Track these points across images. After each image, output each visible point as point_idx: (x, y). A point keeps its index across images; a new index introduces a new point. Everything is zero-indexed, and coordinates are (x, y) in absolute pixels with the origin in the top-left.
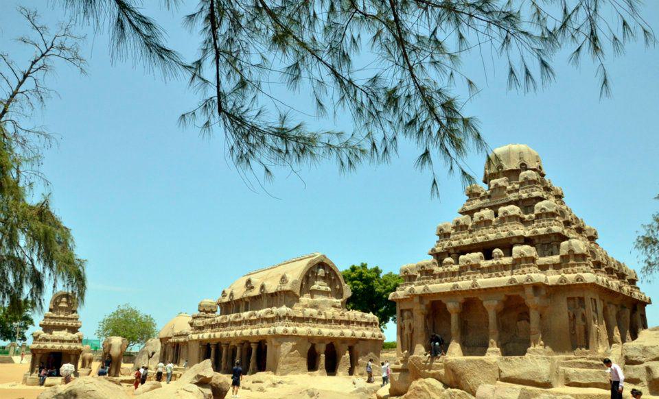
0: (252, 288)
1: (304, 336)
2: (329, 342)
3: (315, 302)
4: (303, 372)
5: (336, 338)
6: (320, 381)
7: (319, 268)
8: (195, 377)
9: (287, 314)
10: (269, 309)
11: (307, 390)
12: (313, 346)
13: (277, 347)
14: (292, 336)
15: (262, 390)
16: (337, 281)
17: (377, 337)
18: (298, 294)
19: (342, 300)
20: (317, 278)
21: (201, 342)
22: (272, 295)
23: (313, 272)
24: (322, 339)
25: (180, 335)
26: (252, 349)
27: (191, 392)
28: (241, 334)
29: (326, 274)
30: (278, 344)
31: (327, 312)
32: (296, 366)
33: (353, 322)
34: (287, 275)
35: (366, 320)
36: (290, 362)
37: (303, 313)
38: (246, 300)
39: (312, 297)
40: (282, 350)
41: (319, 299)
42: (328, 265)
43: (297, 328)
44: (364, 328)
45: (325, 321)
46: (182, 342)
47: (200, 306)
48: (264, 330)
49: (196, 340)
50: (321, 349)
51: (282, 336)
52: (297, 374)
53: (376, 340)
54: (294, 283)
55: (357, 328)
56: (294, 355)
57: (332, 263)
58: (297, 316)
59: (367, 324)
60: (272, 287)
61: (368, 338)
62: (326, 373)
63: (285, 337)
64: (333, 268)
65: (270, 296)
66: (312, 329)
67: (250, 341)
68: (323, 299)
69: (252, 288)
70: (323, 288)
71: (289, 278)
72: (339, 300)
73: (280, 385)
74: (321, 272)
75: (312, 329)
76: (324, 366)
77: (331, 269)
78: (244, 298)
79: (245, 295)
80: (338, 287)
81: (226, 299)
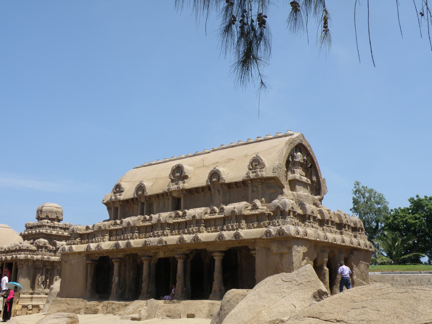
20: (295, 164)
21: (88, 254)
22: (230, 186)
30: (286, 250)
38: (175, 195)
39: (293, 189)
40: (295, 259)
45: (322, 222)
46: (22, 260)
47: (40, 211)
49: (80, 253)
53: (367, 251)
57: (309, 146)
64: (311, 152)
65: (226, 188)
67: (209, 249)
68: (305, 194)
69: (186, 177)
70: (304, 179)
74: (299, 157)
78: (171, 192)
79: (174, 187)
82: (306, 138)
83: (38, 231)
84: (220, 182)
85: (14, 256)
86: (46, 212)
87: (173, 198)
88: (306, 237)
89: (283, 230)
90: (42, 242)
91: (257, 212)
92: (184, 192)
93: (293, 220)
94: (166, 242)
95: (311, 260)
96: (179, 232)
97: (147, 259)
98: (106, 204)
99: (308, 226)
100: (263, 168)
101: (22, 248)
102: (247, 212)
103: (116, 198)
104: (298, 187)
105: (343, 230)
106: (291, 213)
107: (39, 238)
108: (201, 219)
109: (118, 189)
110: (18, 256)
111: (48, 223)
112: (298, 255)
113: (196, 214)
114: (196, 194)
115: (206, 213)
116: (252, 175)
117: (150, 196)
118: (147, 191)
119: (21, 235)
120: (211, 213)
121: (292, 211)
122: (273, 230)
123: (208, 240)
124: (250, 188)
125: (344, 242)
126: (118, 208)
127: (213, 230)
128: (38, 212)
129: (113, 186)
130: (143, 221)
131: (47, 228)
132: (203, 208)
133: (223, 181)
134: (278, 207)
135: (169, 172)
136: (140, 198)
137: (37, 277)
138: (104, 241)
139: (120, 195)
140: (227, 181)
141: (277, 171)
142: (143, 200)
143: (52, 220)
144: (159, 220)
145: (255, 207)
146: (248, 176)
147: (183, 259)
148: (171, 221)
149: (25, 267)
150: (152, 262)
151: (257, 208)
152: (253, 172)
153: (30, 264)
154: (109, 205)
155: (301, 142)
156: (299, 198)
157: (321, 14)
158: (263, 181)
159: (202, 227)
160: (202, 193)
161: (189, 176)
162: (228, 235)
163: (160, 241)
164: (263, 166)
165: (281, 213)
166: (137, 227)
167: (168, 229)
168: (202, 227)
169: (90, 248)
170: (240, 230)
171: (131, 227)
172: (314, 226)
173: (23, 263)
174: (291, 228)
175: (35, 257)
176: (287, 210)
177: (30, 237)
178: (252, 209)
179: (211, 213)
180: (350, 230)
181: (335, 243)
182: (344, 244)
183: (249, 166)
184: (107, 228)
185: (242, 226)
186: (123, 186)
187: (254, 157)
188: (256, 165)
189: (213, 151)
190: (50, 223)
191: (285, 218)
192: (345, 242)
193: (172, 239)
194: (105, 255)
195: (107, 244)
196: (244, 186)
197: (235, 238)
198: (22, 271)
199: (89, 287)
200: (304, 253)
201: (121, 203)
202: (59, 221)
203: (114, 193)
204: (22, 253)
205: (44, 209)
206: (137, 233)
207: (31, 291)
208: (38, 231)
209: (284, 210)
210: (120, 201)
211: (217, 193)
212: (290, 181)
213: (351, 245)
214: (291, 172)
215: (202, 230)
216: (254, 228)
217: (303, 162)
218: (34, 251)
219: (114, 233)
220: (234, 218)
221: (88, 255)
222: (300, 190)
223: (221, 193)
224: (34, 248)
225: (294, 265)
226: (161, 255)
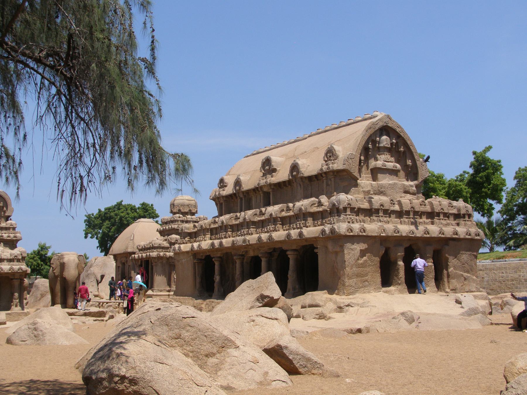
0: (274, 170)
1: (375, 237)
3: (382, 186)
4: (376, 290)
6: (397, 300)
7: (381, 135)
8: (258, 300)
9: (349, 204)
10: (313, 199)
11: (403, 314)
13: (336, 253)
14: (359, 236)
15: (322, 317)
16: (408, 155)
17: (473, 236)
18: (356, 174)
19: (416, 182)
20: (380, 150)
21: (194, 254)
22: (310, 178)
23: (374, 142)
25: (149, 248)
26: (289, 259)
27: (276, 319)
28: (270, 237)
29: (392, 144)
30: (338, 249)
31: (403, 201)
32: (367, 281)
33: (438, 214)
34: (336, 147)
35: (455, 211)
36: (358, 276)
37: (370, 202)
38: (265, 190)
39: (375, 179)
40: (347, 257)
41: (385, 180)
42: (394, 131)
43: (366, 225)
44: (454, 222)
45: (400, 214)
47: (173, 205)
48: (311, 231)
49: (187, 252)
51: (346, 236)
52: (369, 292)
53: (472, 240)
54: (350, 158)
55: (444, 222)
56: (363, 265)
57: (399, 127)
58: (362, 206)
59: (457, 216)
60: (310, 166)
62: (406, 290)
65: (307, 181)
66: (386, 226)
67: (285, 247)
68: (391, 182)
69: (274, 170)
70: (390, 165)
71: (339, 151)
72: (412, 183)
74: (385, 140)
75: (386, 226)
76: (403, 279)
77: (398, 136)
78: (261, 187)
79: (263, 182)
80: (409, 162)
81: (229, 190)
82: (393, 119)
83: (170, 226)
84: (299, 176)
85: (148, 254)
86: (178, 206)
87: (264, 193)
88: (364, 234)
89: (334, 228)
90: (174, 239)
91: (321, 209)
92: (272, 187)
93: (351, 216)
94: (249, 241)
95: (375, 256)
96: (262, 230)
97: (239, 257)
98: (213, 199)
99: (374, 221)
100: (336, 159)
101: (154, 245)
102: (315, 209)
103: (219, 194)
104: (380, 176)
105: (436, 220)
106: (348, 210)
107: (171, 234)
108: (277, 218)
109: (222, 184)
110: (151, 254)
111: (179, 217)
112: (353, 252)
113: (273, 212)
114: (285, 187)
115: (283, 210)
116: (325, 168)
117: (248, 190)
118: (243, 186)
119: (157, 231)
120: (287, 211)
121: (349, 207)
122: (327, 228)
123: (280, 240)
124: (325, 183)
125: (428, 234)
126: (226, 203)
127: (287, 228)
128: (171, 205)
129: (218, 181)
130: (235, 219)
131: (179, 223)
132: (280, 205)
133: (302, 175)
134: (334, 205)
135: (260, 165)
136: (238, 193)
137: (173, 274)
138: (205, 240)
139: (224, 190)
140: (306, 174)
141: (347, 163)
142: (241, 196)
143: (185, 214)
144: (245, 219)
145: (320, 204)
146: (321, 169)
147: (266, 257)
148: (257, 219)
149: (159, 264)
150: (245, 260)
151: (322, 205)
152: (327, 165)
153: (164, 262)
154: (217, 199)
155: (385, 124)
156: (379, 188)
157: (17, 185)
158: (335, 174)
159: (278, 225)
160: (289, 186)
161: (278, 169)
162: (294, 233)
163: (244, 241)
164: (336, 157)
165: (336, 211)
166: (230, 225)
167: (253, 228)
168: (278, 225)
169: (194, 248)
170: (304, 228)
171: (225, 226)
172: (382, 220)
173: (156, 261)
174: (342, 227)
175: (168, 254)
176: (341, 207)
177: (166, 233)
178: (318, 206)
179: (287, 211)
180: (452, 218)
181: (413, 235)
182: (428, 236)
183: (324, 157)
184: (208, 227)
185: (308, 225)
186: (226, 181)
187: (329, 148)
188: (330, 157)
189: (309, 136)
190: (183, 218)
191: (339, 216)
192: (430, 233)
193: (253, 238)
194: (208, 254)
195: (205, 243)
196: (318, 180)
197: (300, 237)
198: (158, 268)
199: (198, 285)
200: (361, 250)
201: (225, 199)
202: (193, 214)
203: (220, 188)
204: (155, 250)
205: (176, 202)
206: (230, 231)
207: (168, 289)
208: (170, 226)
209: (339, 207)
210: (223, 197)
211: (299, 187)
212: (371, 170)
213: (440, 235)
214: (375, 159)
215: (277, 229)
216: (319, 226)
217: (389, 146)
218: (167, 248)
219: (214, 231)
220: (302, 216)
221: (195, 254)
222: (385, 178)
223: (302, 186)
224: (166, 244)
225: (347, 263)
226: (251, 254)
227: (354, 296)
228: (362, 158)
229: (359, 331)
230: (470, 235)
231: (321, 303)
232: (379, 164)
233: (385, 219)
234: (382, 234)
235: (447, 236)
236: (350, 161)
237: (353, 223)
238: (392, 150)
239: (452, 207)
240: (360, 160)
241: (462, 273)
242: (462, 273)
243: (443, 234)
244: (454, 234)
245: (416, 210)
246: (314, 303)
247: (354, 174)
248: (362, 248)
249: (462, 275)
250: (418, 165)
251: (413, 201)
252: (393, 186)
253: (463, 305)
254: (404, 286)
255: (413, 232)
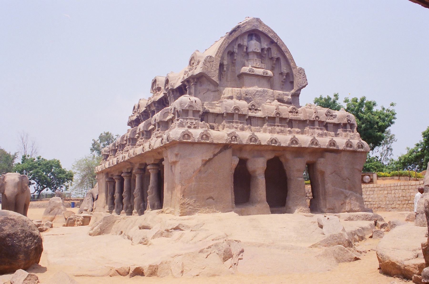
2: (270, 156)
5: (285, 149)
9: (190, 106)
12: (243, 162)
16: (282, 61)
18: (215, 78)
24: (258, 149)
29: (262, 50)
42: (266, 36)
44: (333, 133)
50: (258, 166)
53: (354, 152)
55: (320, 132)
61: (341, 148)
62: (269, 209)
63: (185, 144)
66: (239, 133)
68: (260, 89)
69: (159, 89)
70: (260, 72)
73: (177, 233)
74: (254, 45)
77: (272, 42)
106: (191, 113)
217: (259, 51)
227: (190, 216)
228: (225, 63)
229: (138, 272)
230: (351, 146)
231: (151, 225)
232: (245, 69)
233: (240, 125)
234: (233, 142)
235: (322, 147)
236: (208, 64)
237: (195, 128)
238: (261, 55)
239: (332, 116)
240: (221, 65)
241: (342, 190)
242: (342, 190)
243: (317, 144)
244: (330, 145)
245: (284, 117)
246: (145, 225)
247: (213, 78)
248: (204, 158)
249: (342, 193)
250: (294, 73)
251: (280, 107)
252: (263, 94)
253: (324, 230)
254: (266, 204)
255: (276, 141)
